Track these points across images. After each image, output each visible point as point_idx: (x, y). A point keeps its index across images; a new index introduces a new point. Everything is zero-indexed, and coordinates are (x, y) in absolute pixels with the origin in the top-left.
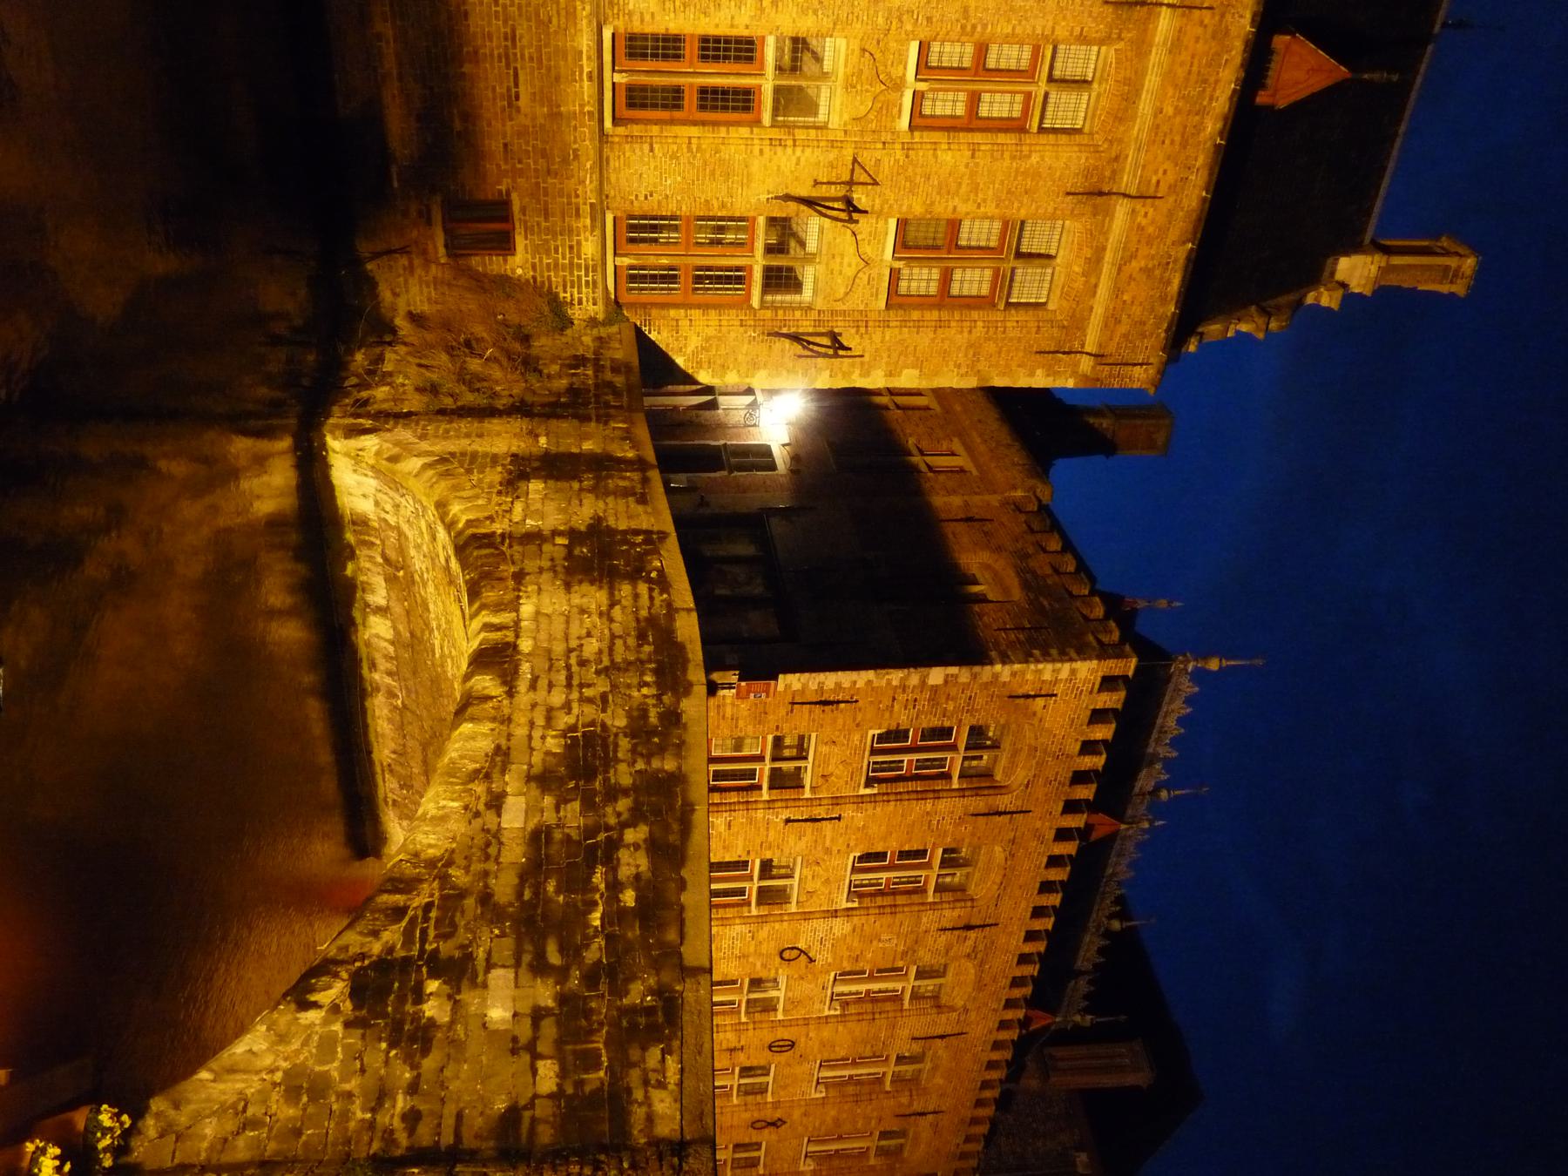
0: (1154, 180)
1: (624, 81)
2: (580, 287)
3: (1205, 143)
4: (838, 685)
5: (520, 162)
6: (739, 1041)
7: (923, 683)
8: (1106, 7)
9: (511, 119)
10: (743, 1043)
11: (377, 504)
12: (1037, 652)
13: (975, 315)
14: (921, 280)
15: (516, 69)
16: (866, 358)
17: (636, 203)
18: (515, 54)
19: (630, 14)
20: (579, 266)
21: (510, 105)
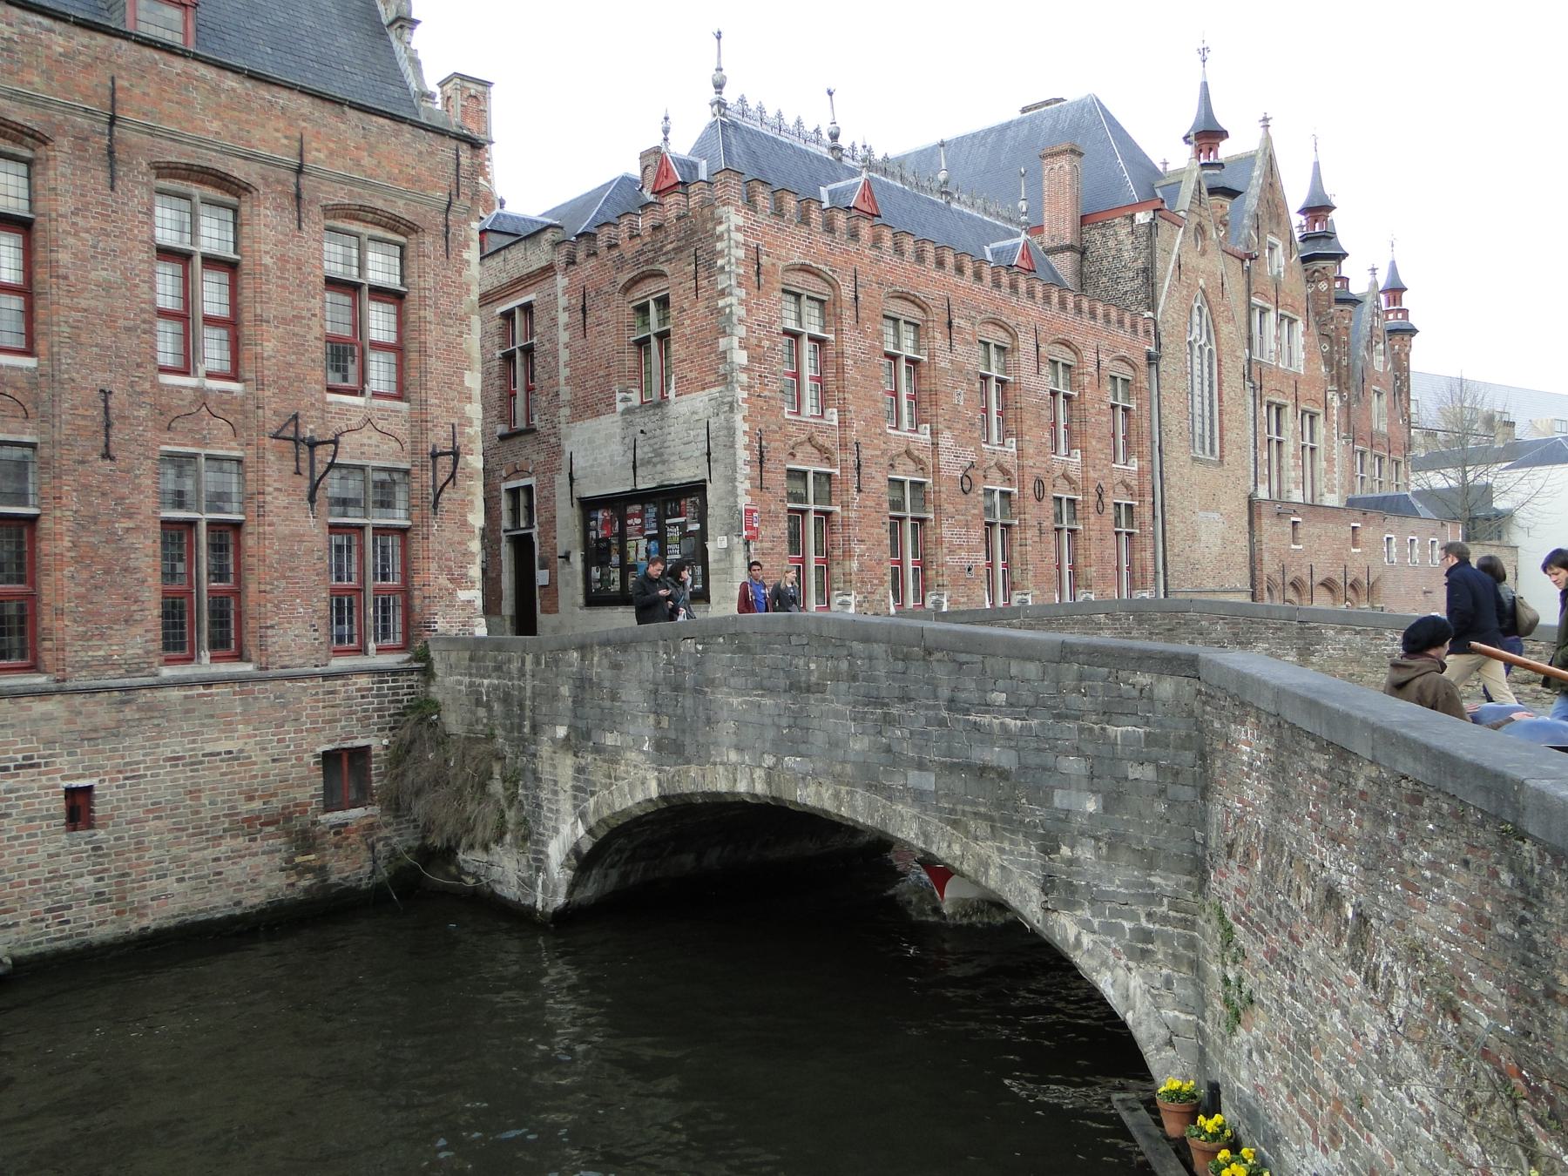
0: (285, 142)
1: (208, 654)
2: (398, 687)
3: (247, 88)
4: (747, 447)
5: (288, 746)
7: (746, 369)
8: (117, 189)
9: (250, 757)
10: (1036, 523)
11: (612, 866)
12: (720, 262)
13: (412, 318)
14: (380, 372)
15: (204, 755)
16: (456, 421)
17: (322, 640)
18: (191, 756)
19: (147, 652)
20: (379, 689)
21: (237, 759)
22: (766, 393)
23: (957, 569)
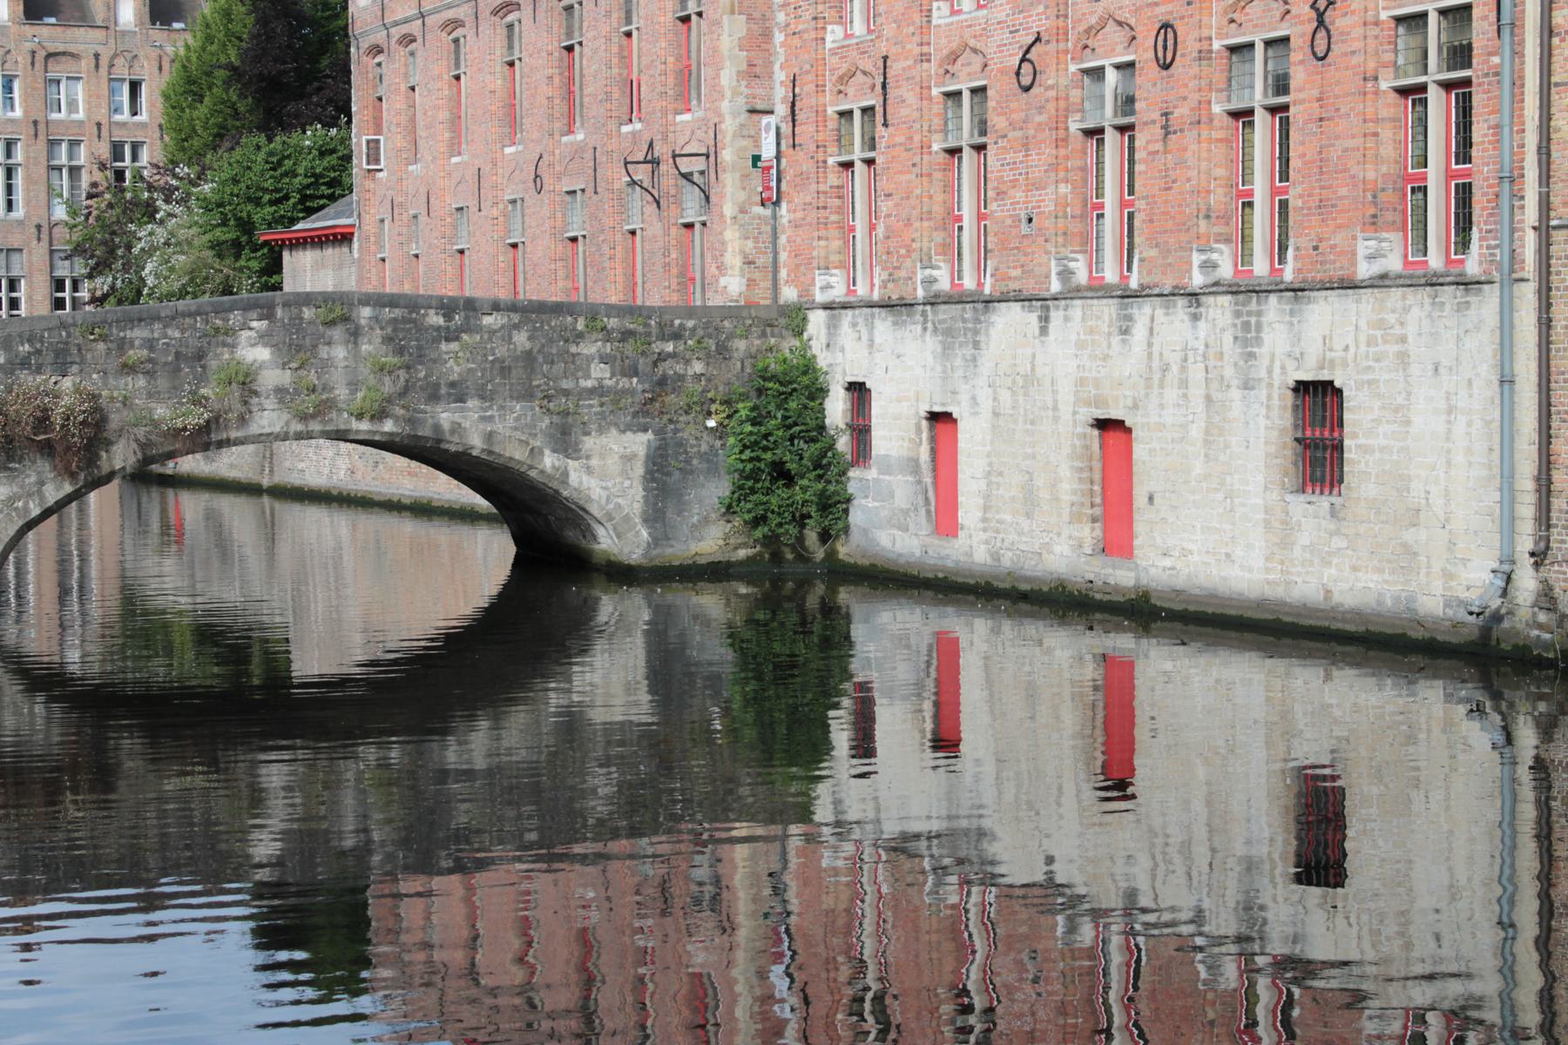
6: (1154, 122)
10: (1156, 115)
16: (716, 120)
22: (801, 27)
23: (1009, 222)
